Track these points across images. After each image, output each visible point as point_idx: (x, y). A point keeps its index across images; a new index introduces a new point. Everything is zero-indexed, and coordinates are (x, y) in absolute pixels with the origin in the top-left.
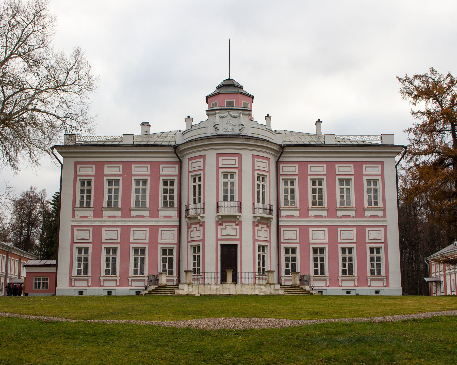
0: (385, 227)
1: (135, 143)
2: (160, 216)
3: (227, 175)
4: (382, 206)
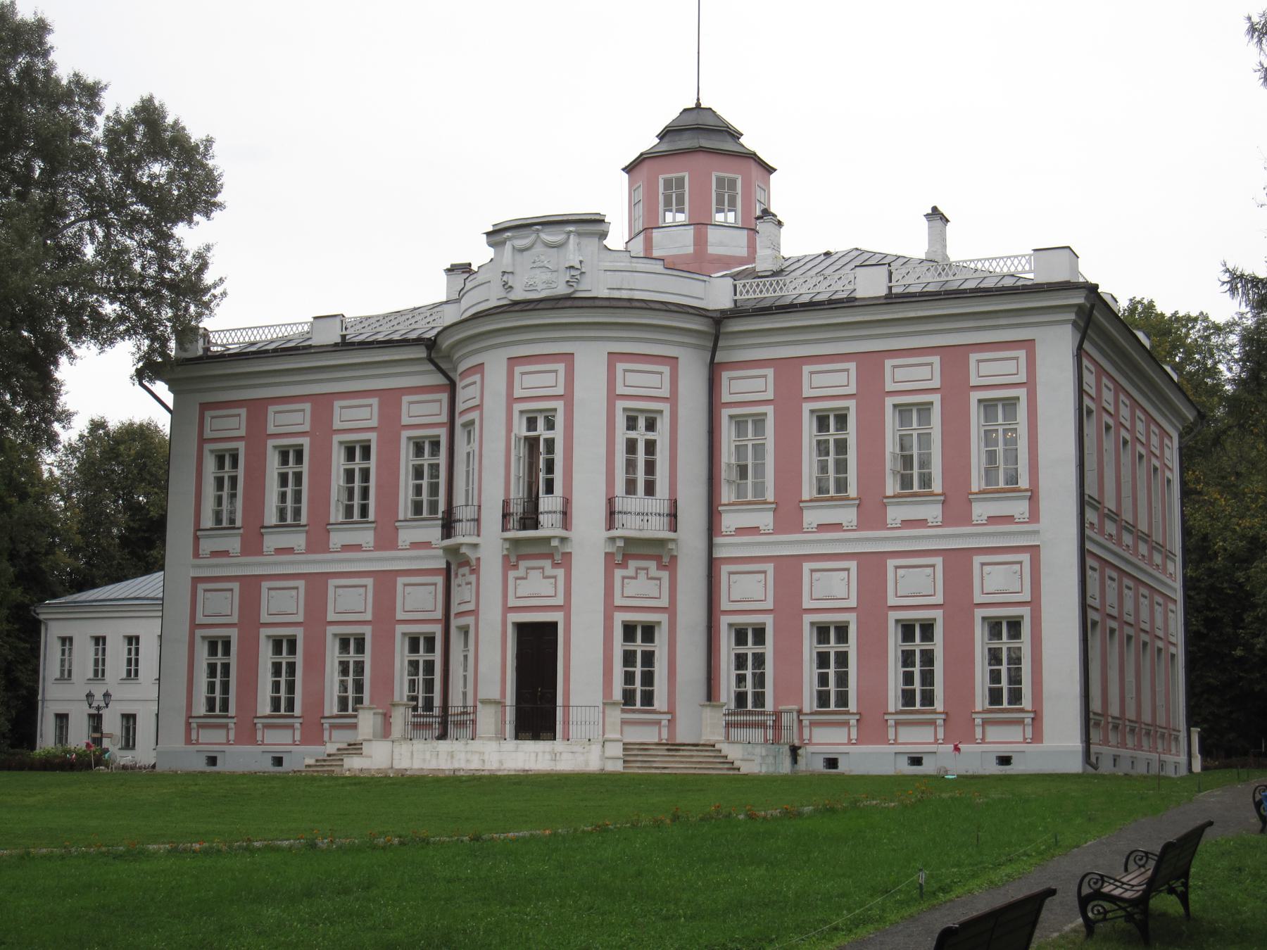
1: (894, 291)
2: (400, 543)
3: (536, 418)
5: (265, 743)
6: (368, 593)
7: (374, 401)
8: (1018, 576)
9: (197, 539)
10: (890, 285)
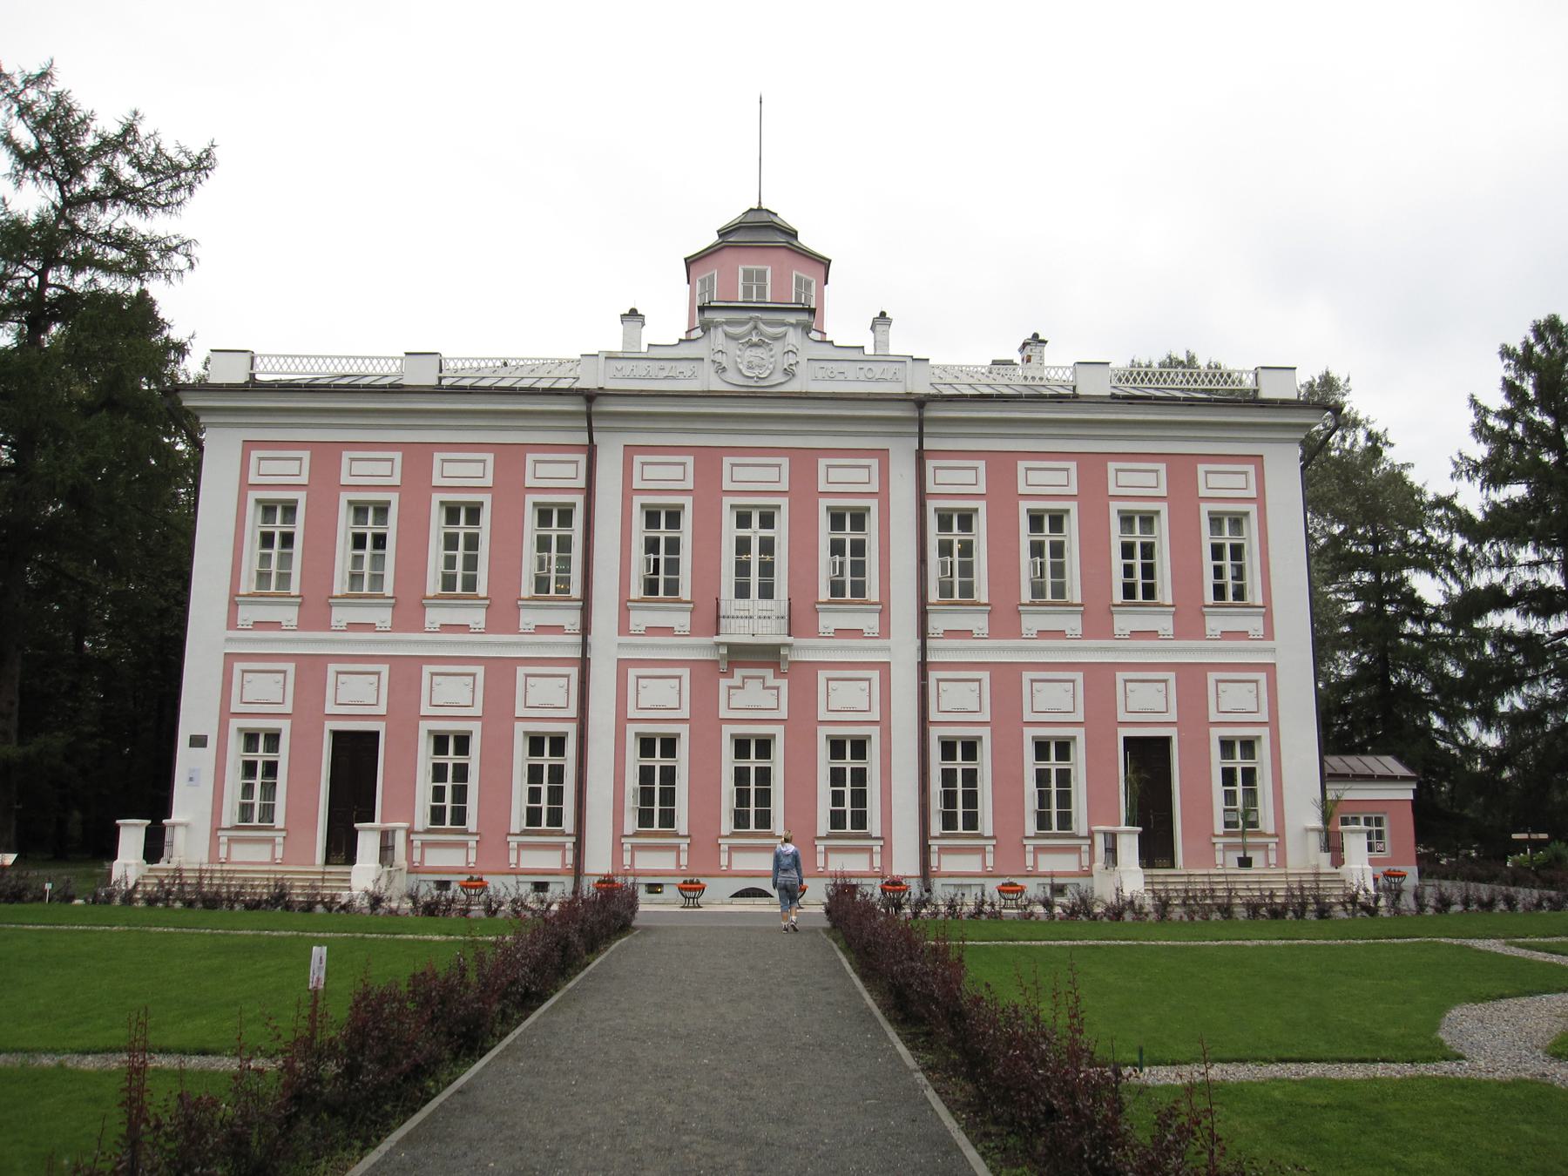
0: (1270, 669)
1: (444, 382)
4: (1259, 602)
5: (232, 860)
6: (288, 681)
7: (306, 455)
8: (564, 690)
9: (234, 605)
10: (441, 375)
